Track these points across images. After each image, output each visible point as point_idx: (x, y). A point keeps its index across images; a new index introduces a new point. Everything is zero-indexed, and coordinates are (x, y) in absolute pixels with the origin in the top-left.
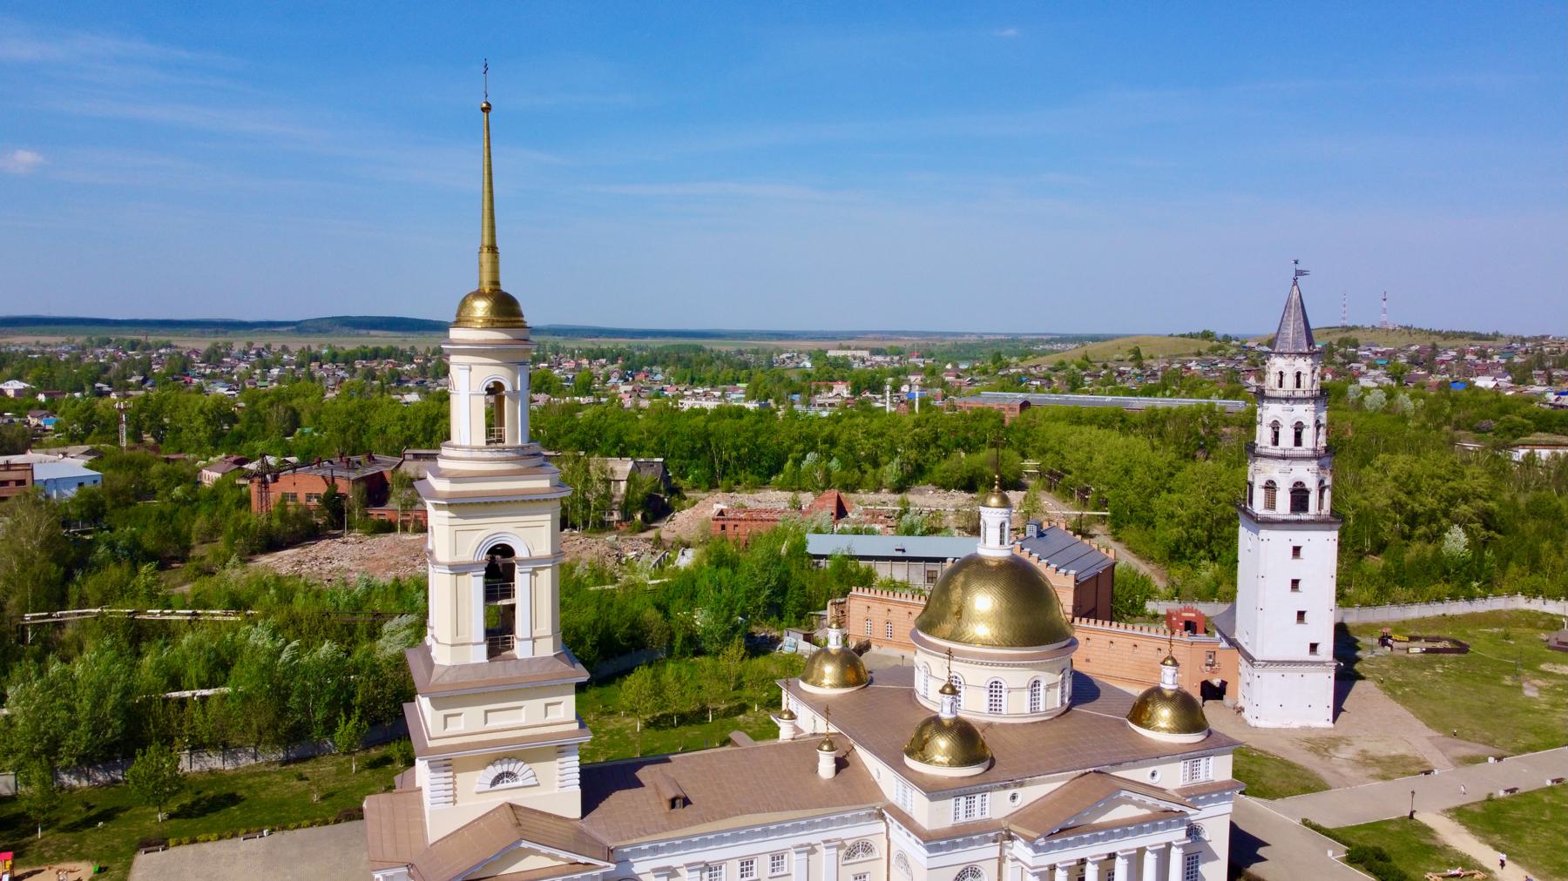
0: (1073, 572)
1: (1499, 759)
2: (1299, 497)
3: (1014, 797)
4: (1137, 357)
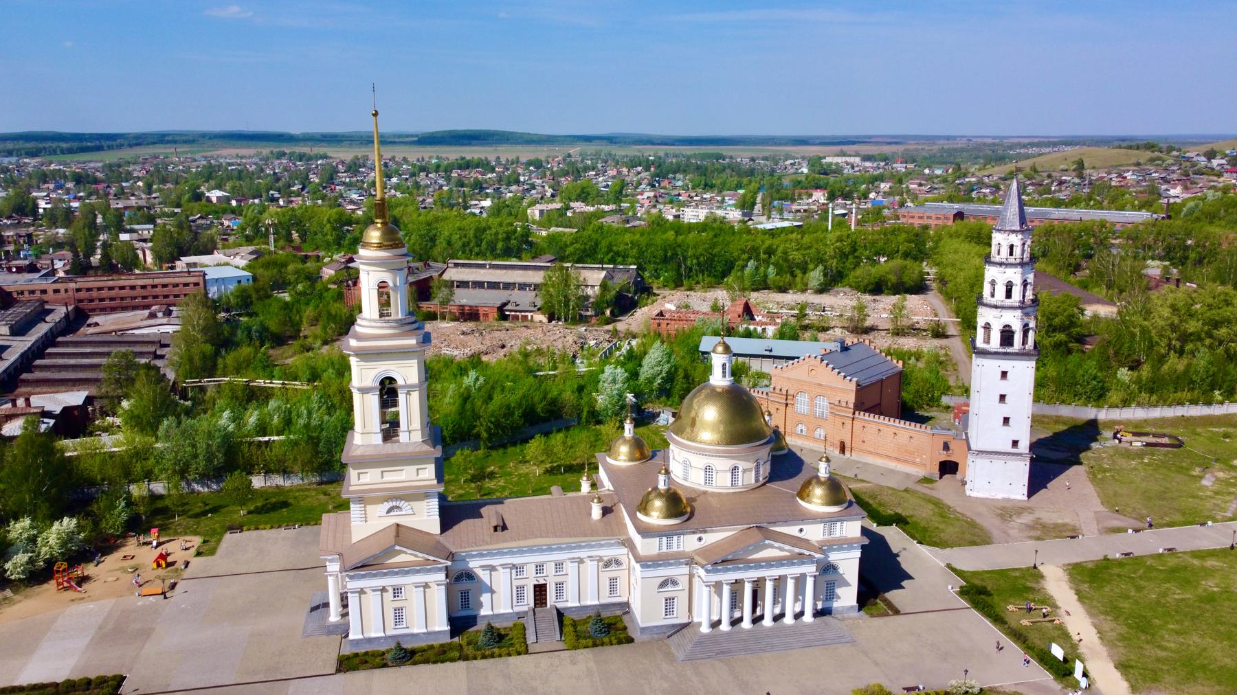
0: (855, 379)
1: (1137, 531)
2: (1007, 336)
3: (700, 539)
4: (1080, 165)
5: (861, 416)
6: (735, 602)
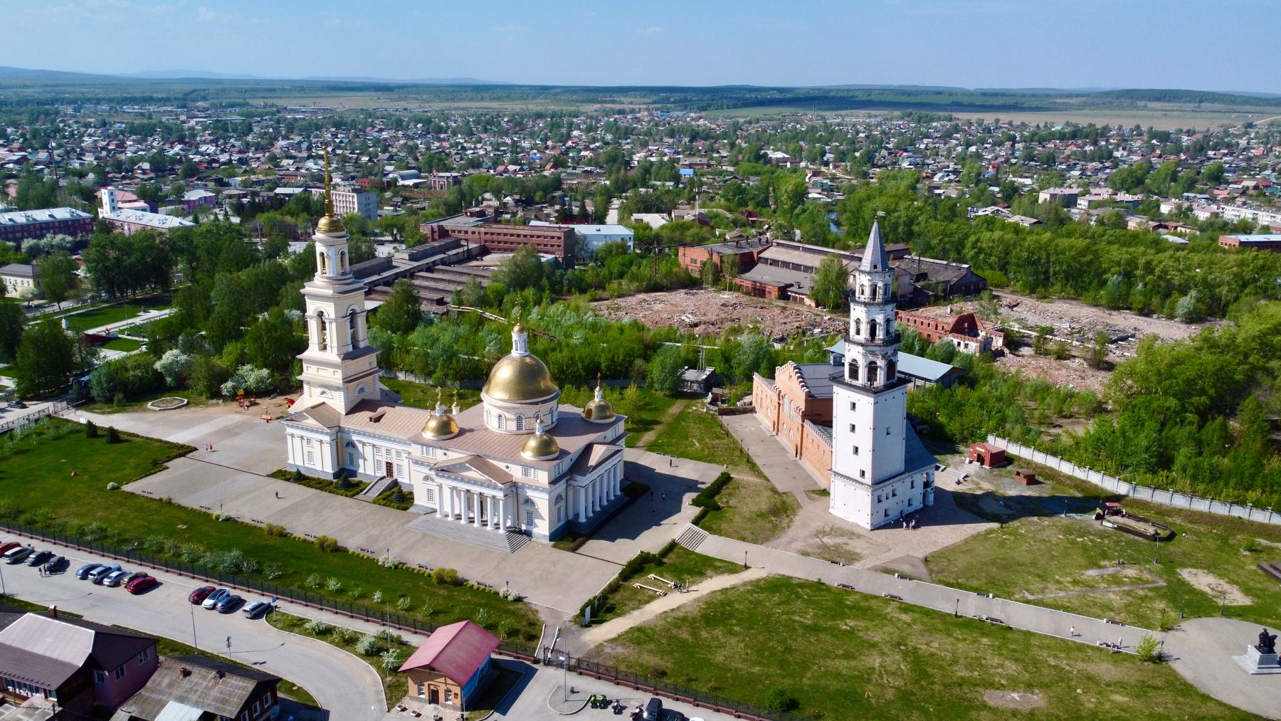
5: (808, 424)
6: (469, 507)
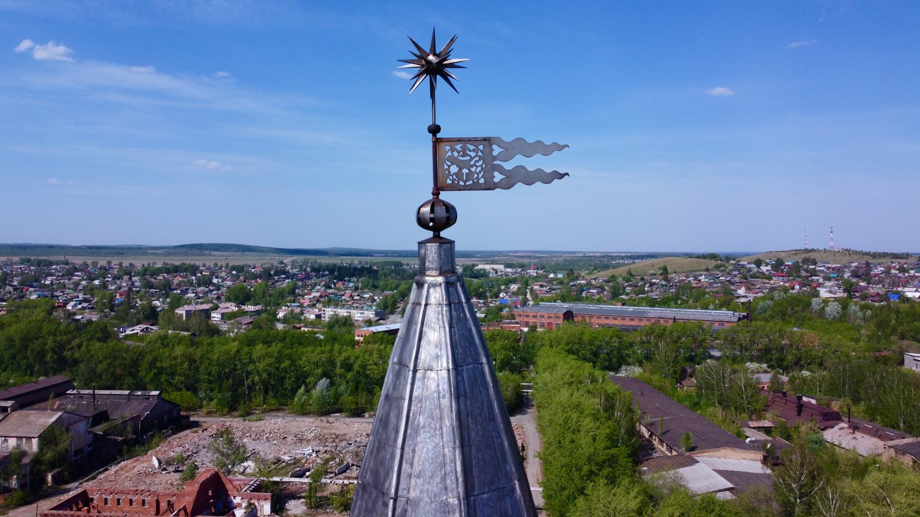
4: (665, 271)
